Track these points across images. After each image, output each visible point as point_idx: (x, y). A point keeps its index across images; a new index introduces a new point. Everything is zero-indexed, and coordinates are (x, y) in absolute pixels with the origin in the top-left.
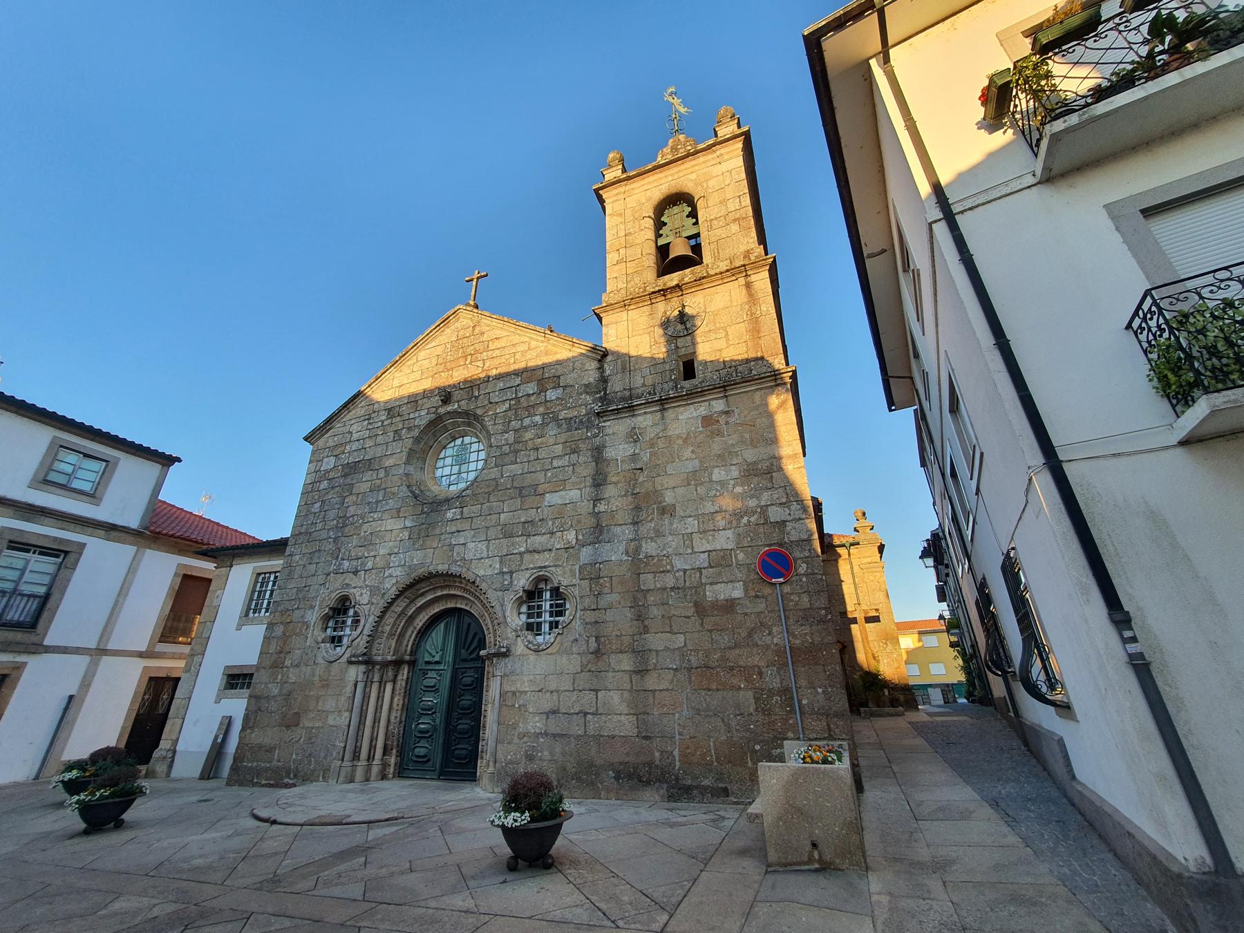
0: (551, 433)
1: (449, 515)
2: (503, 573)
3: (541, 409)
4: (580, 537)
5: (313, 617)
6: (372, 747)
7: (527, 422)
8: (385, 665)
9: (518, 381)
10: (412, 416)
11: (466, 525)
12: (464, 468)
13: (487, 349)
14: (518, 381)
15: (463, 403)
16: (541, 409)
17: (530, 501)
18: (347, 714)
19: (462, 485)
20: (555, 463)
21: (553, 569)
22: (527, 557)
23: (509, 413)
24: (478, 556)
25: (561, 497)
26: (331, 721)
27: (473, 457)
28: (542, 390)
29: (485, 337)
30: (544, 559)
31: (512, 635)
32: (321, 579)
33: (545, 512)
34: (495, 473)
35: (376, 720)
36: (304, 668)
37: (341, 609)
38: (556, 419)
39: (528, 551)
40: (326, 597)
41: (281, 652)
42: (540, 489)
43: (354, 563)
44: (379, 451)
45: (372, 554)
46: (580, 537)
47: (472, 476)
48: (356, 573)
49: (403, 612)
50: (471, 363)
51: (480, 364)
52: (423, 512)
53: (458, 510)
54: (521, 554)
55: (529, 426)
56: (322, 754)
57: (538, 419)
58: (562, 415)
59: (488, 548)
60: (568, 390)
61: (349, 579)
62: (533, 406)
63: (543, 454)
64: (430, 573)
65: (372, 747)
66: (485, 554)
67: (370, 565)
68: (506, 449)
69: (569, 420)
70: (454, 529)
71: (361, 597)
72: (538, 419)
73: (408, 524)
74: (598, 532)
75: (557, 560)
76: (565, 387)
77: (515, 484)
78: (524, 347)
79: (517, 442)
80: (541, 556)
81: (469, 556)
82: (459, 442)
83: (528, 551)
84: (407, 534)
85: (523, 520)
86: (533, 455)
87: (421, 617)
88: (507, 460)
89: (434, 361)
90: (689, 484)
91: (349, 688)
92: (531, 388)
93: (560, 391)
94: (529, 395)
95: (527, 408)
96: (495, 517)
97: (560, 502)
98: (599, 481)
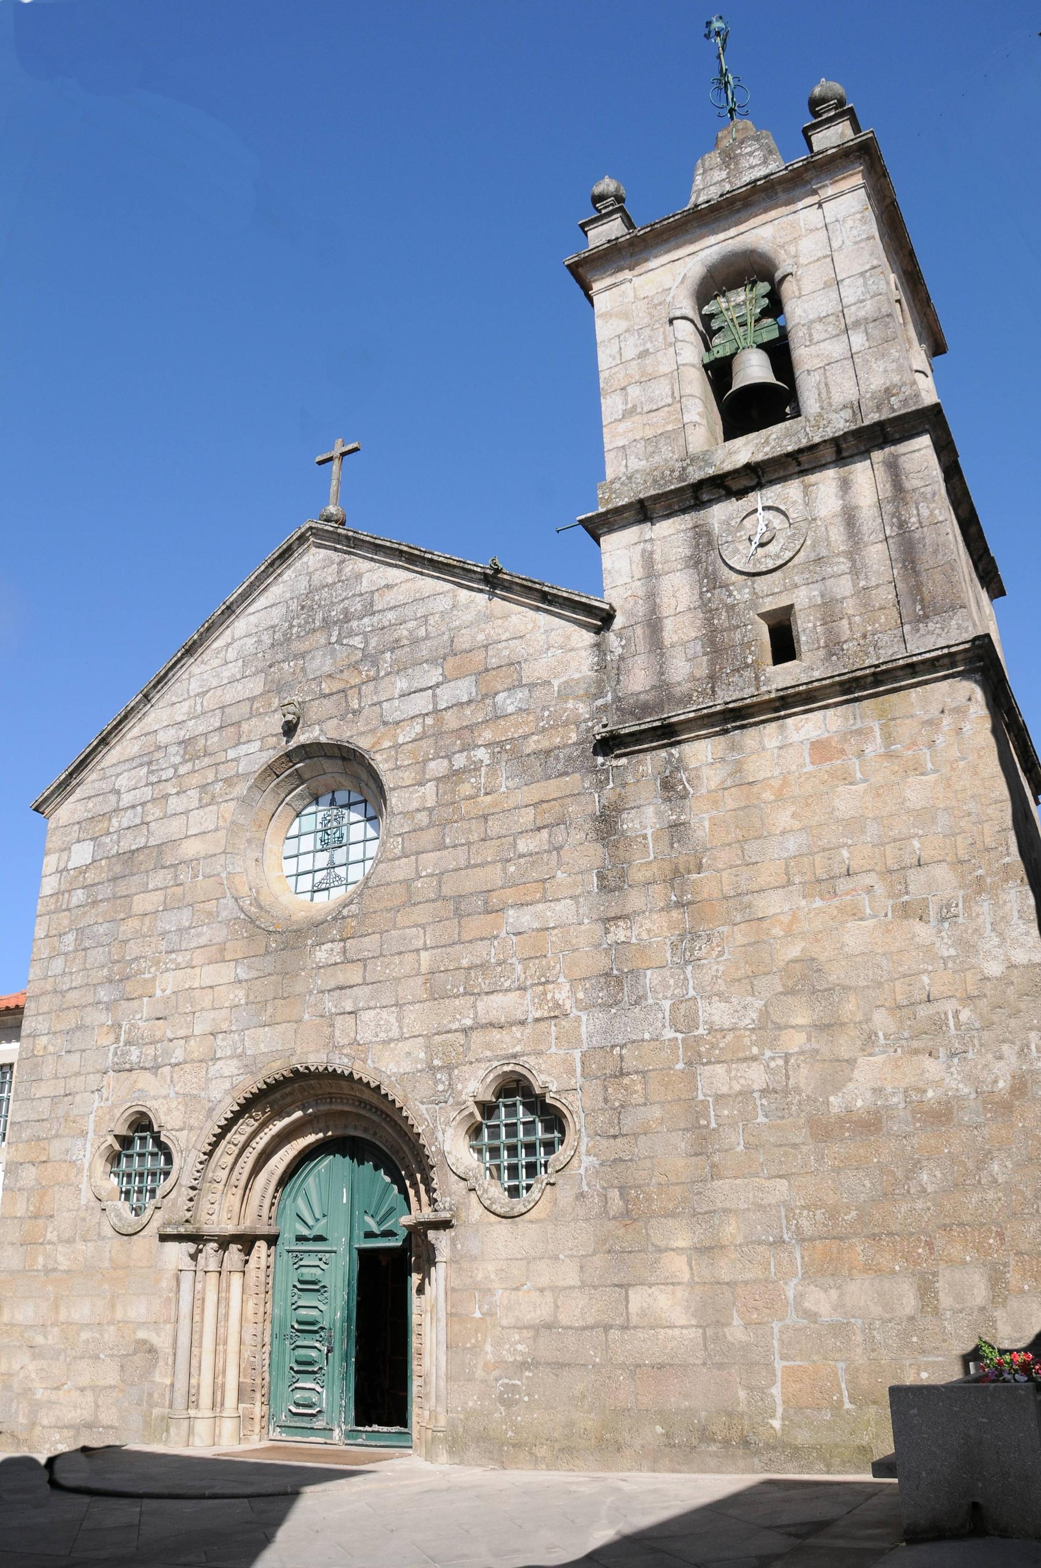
1: (321, 955)
2: (432, 1069)
4: (581, 995)
5: (89, 1152)
6: (218, 1388)
7: (460, 761)
8: (224, 1242)
9: (434, 675)
10: (232, 754)
11: (353, 974)
12: (340, 856)
13: (369, 610)
14: (434, 675)
16: (488, 735)
17: (475, 926)
18: (169, 1327)
19: (338, 893)
20: (524, 845)
23: (424, 743)
24: (383, 1036)
29: (365, 586)
30: (512, 1041)
32: (93, 1081)
34: (403, 869)
35: (220, 1341)
36: (80, 1246)
37: (139, 1139)
40: (102, 1117)
41: (35, 1217)
42: (495, 900)
43: (150, 1051)
44: (174, 828)
45: (181, 1033)
47: (356, 873)
48: (155, 1069)
49: (246, 1144)
50: (339, 641)
51: (357, 641)
52: (267, 953)
53: (338, 946)
54: (465, 1031)
55: (464, 770)
57: (482, 754)
58: (532, 745)
59: (399, 1020)
60: (538, 692)
61: (145, 1080)
62: (470, 728)
63: (495, 827)
64: (296, 1072)
65: (218, 1388)
66: (395, 1033)
67: (178, 1055)
68: (423, 818)
70: (332, 984)
71: (168, 1118)
72: (482, 754)
73: (242, 974)
74: (615, 983)
76: (532, 686)
77: (446, 891)
78: (442, 604)
81: (365, 1035)
84: (240, 995)
85: (465, 963)
87: (281, 1153)
89: (267, 639)
90: (790, 883)
91: (166, 1283)
92: (463, 689)
93: (521, 694)
95: (458, 732)
96: (409, 958)
98: (611, 882)
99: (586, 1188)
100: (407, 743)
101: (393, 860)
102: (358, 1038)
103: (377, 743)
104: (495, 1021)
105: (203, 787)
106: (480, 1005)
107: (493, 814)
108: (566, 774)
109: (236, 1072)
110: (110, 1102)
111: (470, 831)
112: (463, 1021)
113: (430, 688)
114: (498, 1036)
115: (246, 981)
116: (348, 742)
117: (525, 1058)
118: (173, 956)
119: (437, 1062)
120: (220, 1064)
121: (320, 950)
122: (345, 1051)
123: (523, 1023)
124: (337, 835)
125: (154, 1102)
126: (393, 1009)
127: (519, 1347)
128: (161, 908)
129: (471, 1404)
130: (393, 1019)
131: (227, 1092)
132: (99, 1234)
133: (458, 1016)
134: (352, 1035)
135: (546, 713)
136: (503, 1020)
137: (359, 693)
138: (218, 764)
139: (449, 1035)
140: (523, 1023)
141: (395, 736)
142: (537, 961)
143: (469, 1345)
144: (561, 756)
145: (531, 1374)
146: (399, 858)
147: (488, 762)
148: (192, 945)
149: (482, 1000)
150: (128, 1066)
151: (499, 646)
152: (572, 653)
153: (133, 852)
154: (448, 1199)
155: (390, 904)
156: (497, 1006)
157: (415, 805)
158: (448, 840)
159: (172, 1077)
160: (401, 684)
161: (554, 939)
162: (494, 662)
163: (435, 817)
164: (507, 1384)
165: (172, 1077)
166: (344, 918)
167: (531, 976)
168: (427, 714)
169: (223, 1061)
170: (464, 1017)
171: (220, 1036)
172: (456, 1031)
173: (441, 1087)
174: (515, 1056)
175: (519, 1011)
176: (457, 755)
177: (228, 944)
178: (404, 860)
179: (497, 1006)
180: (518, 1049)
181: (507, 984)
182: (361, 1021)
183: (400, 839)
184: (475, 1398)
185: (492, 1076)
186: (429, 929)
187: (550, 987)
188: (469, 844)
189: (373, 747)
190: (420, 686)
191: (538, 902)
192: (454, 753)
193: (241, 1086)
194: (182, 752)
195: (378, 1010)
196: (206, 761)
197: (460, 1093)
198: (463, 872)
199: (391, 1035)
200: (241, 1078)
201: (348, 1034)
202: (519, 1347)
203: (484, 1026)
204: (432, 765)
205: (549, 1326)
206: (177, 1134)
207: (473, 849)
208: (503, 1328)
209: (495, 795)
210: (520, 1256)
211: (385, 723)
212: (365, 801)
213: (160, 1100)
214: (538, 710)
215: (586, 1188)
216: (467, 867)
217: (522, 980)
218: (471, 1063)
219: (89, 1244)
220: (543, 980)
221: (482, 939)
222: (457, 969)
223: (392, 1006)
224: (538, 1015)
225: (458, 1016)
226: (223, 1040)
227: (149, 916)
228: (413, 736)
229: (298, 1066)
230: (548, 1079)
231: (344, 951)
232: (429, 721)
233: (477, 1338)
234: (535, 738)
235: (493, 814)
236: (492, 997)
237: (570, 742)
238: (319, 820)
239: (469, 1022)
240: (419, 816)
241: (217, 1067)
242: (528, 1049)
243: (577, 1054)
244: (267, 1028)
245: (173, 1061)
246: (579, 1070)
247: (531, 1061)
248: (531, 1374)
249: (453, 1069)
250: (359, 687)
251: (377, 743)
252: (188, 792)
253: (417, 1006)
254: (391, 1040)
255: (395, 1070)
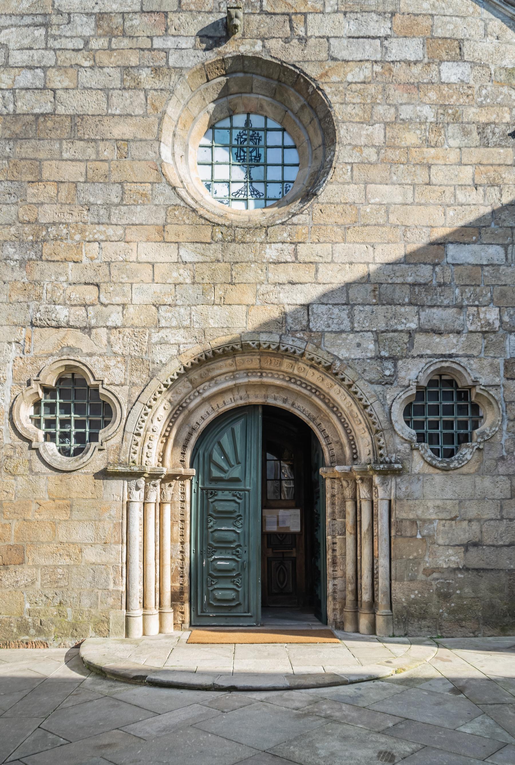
0: (453, 143)
1: (271, 252)
2: (380, 358)
3: (433, 95)
7: (406, 112)
15: (271, 44)
20: (461, 197)
21: (464, 361)
22: (420, 338)
23: (372, 89)
25: (474, 253)
26: (91, 555)
27: (274, 156)
28: (433, 60)
31: (404, 448)
33: (447, 275)
38: (456, 119)
39: (421, 330)
46: (506, 319)
54: (410, 333)
56: (86, 602)
59: (351, 317)
68: (371, 154)
69: (482, 129)
70: (283, 278)
72: (428, 113)
75: (470, 347)
76: (473, 64)
79: (390, 145)
80: (444, 340)
82: (239, 120)
83: (421, 330)
85: (410, 280)
86: (422, 176)
88: (374, 173)
94: (408, 63)
97: (472, 260)
99: (505, 454)
100: (356, 83)
101: (343, 184)
102: (311, 326)
103: (326, 74)
104: (435, 328)
105: (126, 69)
106: (423, 314)
107: (436, 165)
108: (500, 146)
109: (184, 341)
110: (32, 354)
111: (415, 174)
112: (408, 325)
113: (379, 37)
114: (438, 340)
115: (190, 263)
116: (294, 66)
117: (459, 359)
118: (102, 228)
119: (383, 353)
120: (163, 333)
121: (270, 248)
122: (298, 335)
123: (459, 333)
124: (254, 154)
125: (88, 358)
126: (345, 307)
127: (453, 558)
128: (82, 179)
129: (413, 596)
130: (344, 315)
131: (172, 358)
132: (31, 470)
133: (404, 321)
134: (304, 323)
135: (484, 92)
136: (443, 328)
137: (305, 22)
138: (143, 50)
139: (396, 334)
140: (459, 333)
141: (345, 75)
142: (472, 288)
143: (411, 557)
144: (497, 130)
145: (462, 576)
146: (348, 183)
147: (433, 120)
148: (124, 221)
149: (423, 311)
150: (54, 324)
151: (445, 19)
152: (508, 46)
153: (37, 116)
154: (394, 455)
155: (340, 221)
156: (437, 316)
157: (363, 141)
158: (395, 178)
159: (109, 338)
160: (350, 27)
161: (486, 274)
162: (439, 33)
163: (381, 156)
164: (442, 582)
165: (109, 338)
166: (293, 224)
167: (468, 299)
168: (376, 62)
169: (168, 330)
170: (409, 321)
171: (163, 308)
172: (402, 331)
173: (387, 373)
174: (451, 356)
175: (456, 324)
176: (403, 107)
177: (168, 228)
178: (353, 187)
179: (437, 316)
180: (453, 351)
181: (446, 302)
182: (313, 313)
183: (349, 167)
184: (416, 592)
185: (432, 368)
186: (379, 248)
187: (483, 309)
188: (414, 185)
189: (321, 77)
190: (368, 34)
191: (474, 243)
192: (401, 104)
193: (189, 353)
194: (93, 25)
195: (331, 306)
196: (125, 43)
197: (404, 378)
198: (408, 207)
199: (342, 327)
200: (189, 346)
201: (300, 322)
202: (453, 558)
203: (426, 331)
204: (380, 109)
205: (475, 545)
206: (117, 388)
207: (418, 189)
208: (439, 545)
209: (439, 149)
210: (453, 497)
211: (334, 59)
212: (283, 130)
213: (95, 358)
214: (477, 87)
215: (505, 454)
216: (412, 204)
217: (459, 300)
218: (413, 357)
219: (19, 478)
220: (477, 303)
221: (425, 264)
222: (403, 284)
223: (343, 304)
224: (472, 328)
225: (404, 321)
226: (166, 311)
227: (66, 185)
228: (361, 78)
229: (251, 343)
230: (478, 375)
231: (296, 253)
232: (377, 68)
233: (418, 552)
234: (473, 110)
235: (436, 165)
236: (434, 310)
237: (504, 121)
238: (235, 136)
239: (413, 326)
240: (367, 151)
241: (160, 334)
242: (461, 353)
243: (500, 362)
244: (215, 307)
245: (109, 324)
246: (502, 372)
247: (464, 361)
248: (462, 576)
249: (398, 360)
250: (305, 14)
251: (326, 74)
252: (106, 70)
253: (367, 308)
254: (342, 332)
255: (347, 355)
